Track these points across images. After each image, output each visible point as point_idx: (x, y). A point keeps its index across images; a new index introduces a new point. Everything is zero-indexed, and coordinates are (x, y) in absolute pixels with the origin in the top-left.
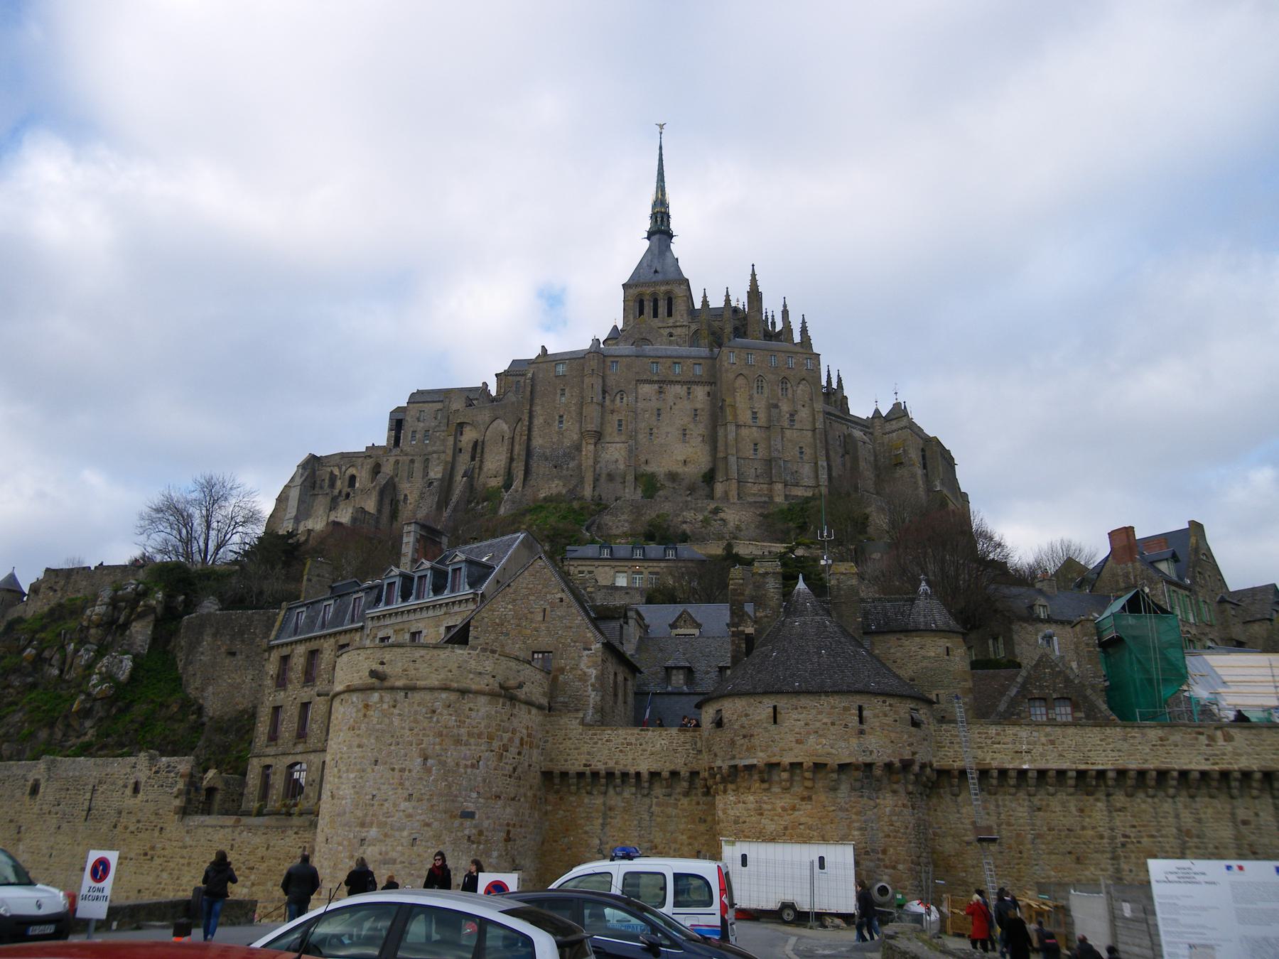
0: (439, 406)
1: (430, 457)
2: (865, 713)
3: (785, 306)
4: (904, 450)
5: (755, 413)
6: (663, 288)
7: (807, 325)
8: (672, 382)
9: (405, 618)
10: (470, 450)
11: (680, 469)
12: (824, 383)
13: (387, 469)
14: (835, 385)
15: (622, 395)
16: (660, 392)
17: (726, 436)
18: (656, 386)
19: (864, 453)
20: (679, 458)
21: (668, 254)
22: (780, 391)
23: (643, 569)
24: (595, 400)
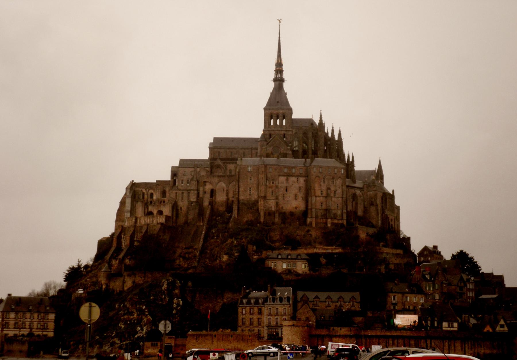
0: (193, 169)
1: (190, 192)
2: (352, 329)
3: (333, 127)
4: (374, 200)
5: (322, 191)
6: (281, 111)
7: (341, 132)
8: (292, 176)
9: (274, 306)
10: (210, 193)
11: (294, 210)
12: (346, 160)
13: (171, 195)
14: (351, 160)
15: (273, 181)
16: (287, 180)
17: (312, 200)
18: (286, 178)
19: (360, 201)
20: (294, 206)
22: (331, 182)
23: (290, 262)
24: (264, 184)
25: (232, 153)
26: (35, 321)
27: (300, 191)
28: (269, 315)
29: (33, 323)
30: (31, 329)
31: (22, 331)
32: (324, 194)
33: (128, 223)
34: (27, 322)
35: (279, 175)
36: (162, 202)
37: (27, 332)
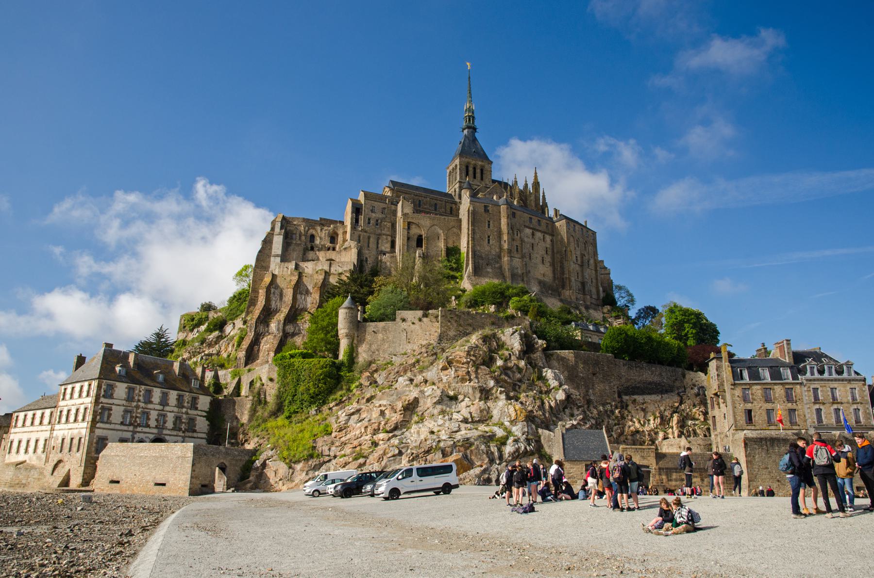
3: (544, 193)
5: (576, 257)
6: (480, 163)
8: (538, 230)
16: (533, 234)
18: (531, 231)
20: (542, 272)
21: (477, 142)
25: (420, 201)
26: (170, 412)
27: (547, 253)
28: (815, 403)
29: (165, 416)
30: (160, 427)
31: (139, 432)
32: (579, 262)
33: (279, 272)
34: (152, 412)
35: (526, 226)
36: (331, 248)
37: (152, 436)
